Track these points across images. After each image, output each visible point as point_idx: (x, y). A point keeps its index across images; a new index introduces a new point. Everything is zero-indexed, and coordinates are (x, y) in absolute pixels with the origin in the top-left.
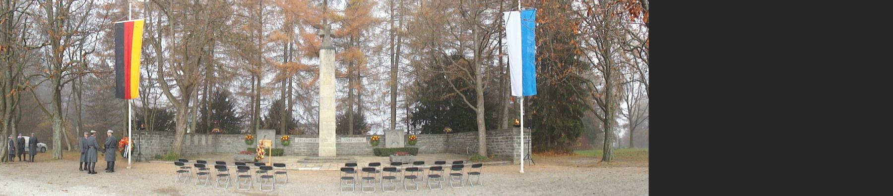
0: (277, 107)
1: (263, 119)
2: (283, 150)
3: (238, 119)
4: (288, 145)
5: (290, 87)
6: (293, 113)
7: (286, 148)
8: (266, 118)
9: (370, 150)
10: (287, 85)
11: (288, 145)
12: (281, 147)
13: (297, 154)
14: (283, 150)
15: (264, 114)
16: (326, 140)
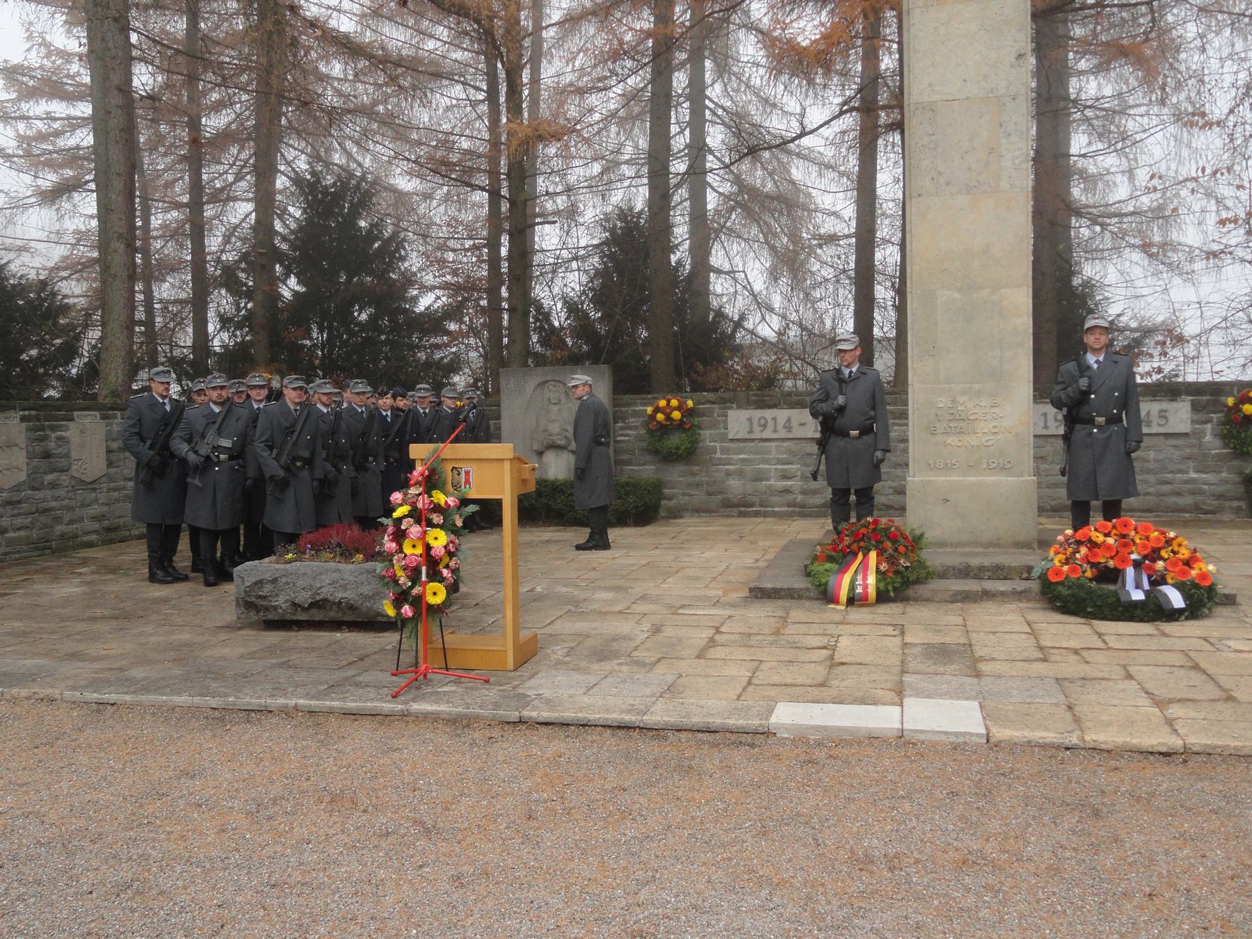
0: (633, 250)
1: (559, 318)
2: (657, 488)
3: (433, 323)
4: (688, 455)
5: (698, 149)
6: (719, 285)
7: (675, 475)
8: (572, 308)
9: (1220, 479)
10: (680, 141)
11: (688, 455)
12: (646, 471)
13: (740, 507)
14: (657, 488)
15: (562, 287)
16: (959, 422)
